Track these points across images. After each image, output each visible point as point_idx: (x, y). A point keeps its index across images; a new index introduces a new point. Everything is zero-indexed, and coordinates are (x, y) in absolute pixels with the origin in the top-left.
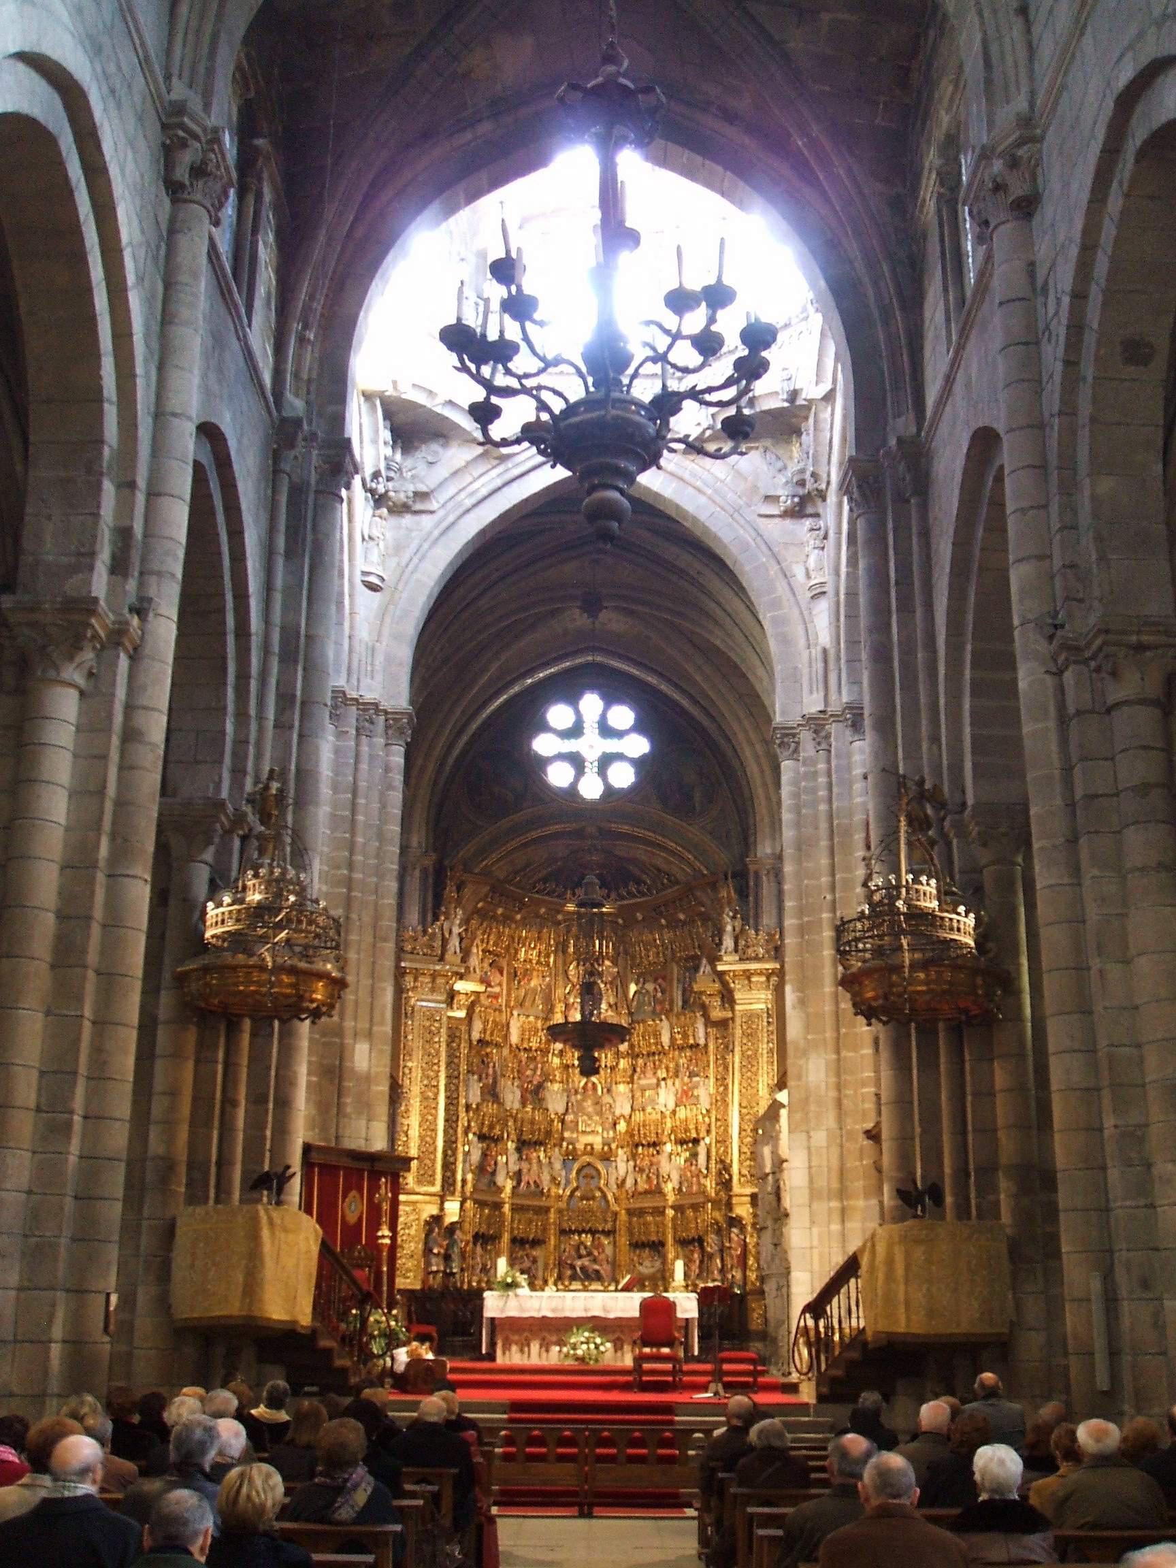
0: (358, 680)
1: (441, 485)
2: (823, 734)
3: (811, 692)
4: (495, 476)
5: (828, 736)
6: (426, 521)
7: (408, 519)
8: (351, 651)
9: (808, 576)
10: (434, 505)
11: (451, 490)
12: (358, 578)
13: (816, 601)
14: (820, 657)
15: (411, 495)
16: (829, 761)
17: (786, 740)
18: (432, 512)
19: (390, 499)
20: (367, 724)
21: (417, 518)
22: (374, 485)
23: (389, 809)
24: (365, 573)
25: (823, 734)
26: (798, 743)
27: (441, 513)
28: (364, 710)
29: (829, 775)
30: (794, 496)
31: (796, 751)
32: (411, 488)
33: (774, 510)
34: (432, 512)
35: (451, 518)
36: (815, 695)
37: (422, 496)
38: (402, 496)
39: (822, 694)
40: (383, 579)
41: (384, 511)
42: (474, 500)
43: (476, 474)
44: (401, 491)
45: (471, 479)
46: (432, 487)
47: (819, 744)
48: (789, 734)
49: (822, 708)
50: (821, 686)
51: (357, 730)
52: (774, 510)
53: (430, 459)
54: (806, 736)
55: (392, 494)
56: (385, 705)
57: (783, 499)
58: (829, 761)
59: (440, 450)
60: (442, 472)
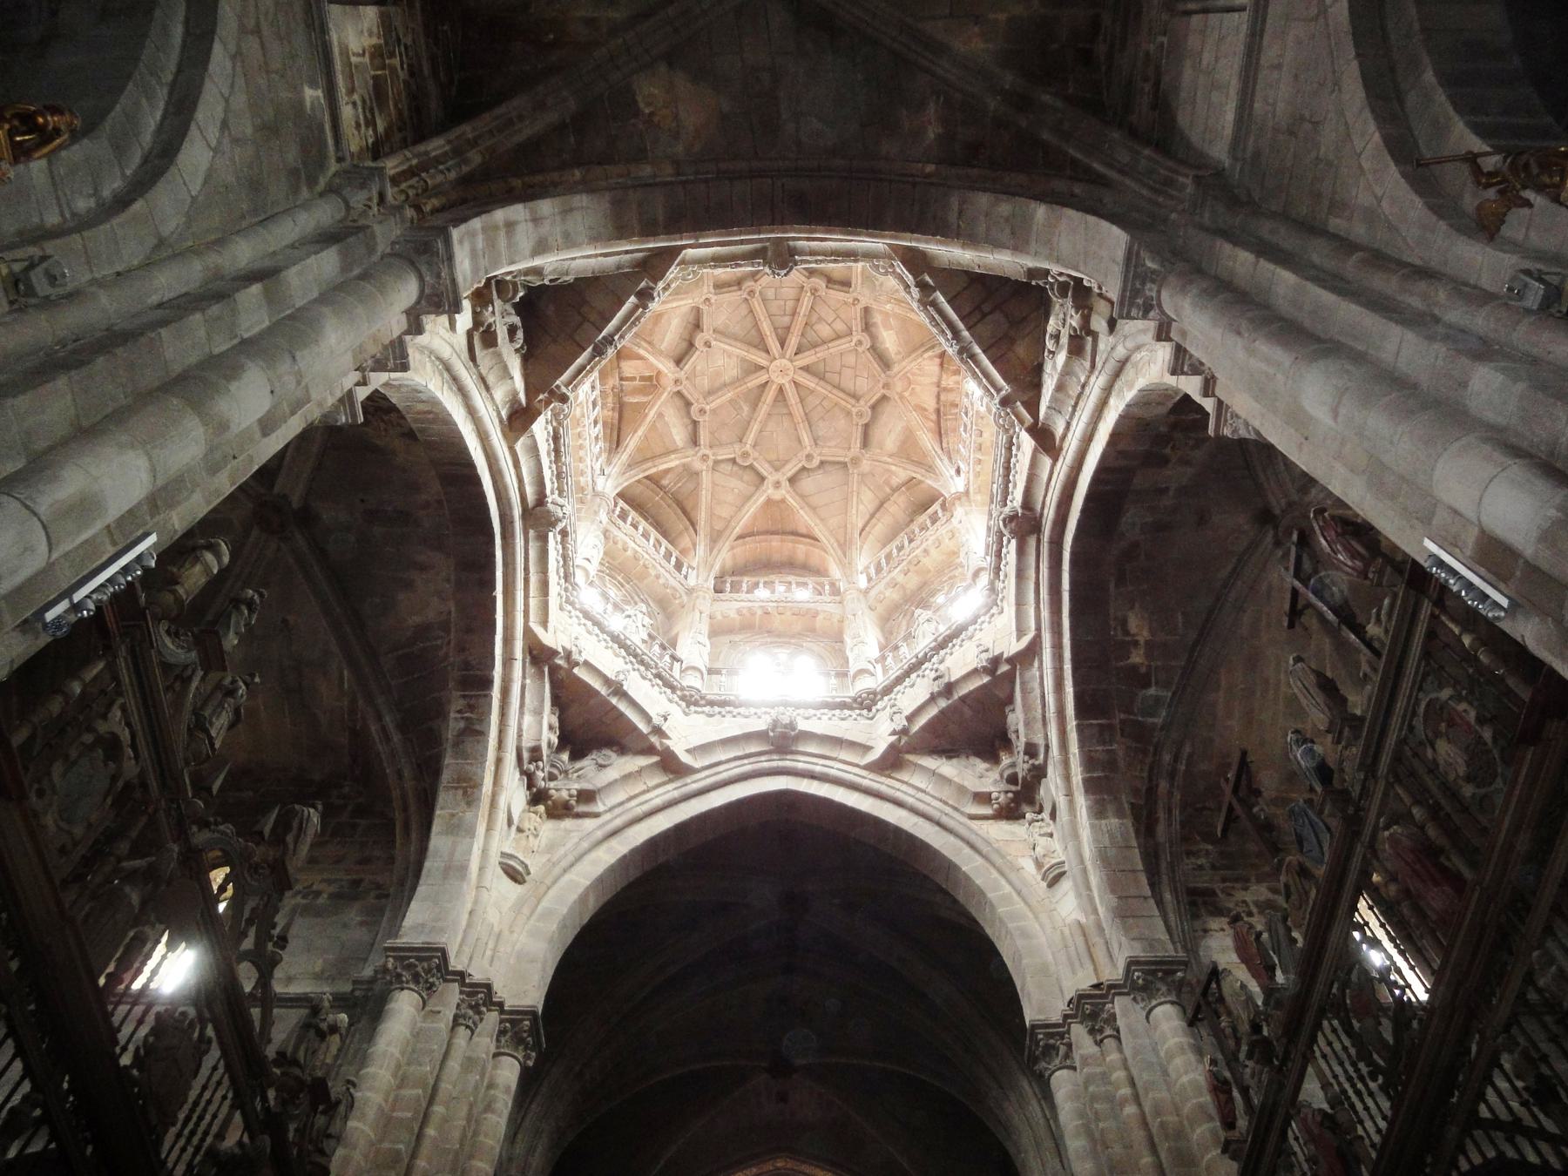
0: (471, 958)
1: (610, 785)
2: (1105, 1015)
3: (1074, 972)
4: (671, 791)
5: (1113, 1017)
6: (589, 824)
7: (568, 823)
8: (469, 925)
9: (1039, 865)
10: (599, 807)
11: (620, 796)
12: (494, 859)
13: (1056, 886)
14: (1078, 933)
15: (575, 793)
16: (1120, 1050)
17: (1052, 1041)
18: (597, 815)
19: (549, 797)
20: (470, 1012)
21: (580, 821)
22: (532, 767)
23: (481, 1138)
24: (503, 855)
25: (1105, 1015)
26: (1069, 1046)
27: (607, 817)
28: (469, 994)
29: (1126, 1068)
30: (1007, 792)
31: (1067, 1056)
32: (576, 786)
33: (988, 811)
34: (597, 815)
35: (618, 822)
36: (1080, 974)
37: (587, 796)
38: (565, 794)
39: (1091, 968)
40: (529, 873)
41: (541, 808)
42: (646, 808)
43: (651, 783)
44: (563, 790)
45: (645, 787)
46: (599, 785)
47: (1101, 1031)
48: (1058, 1032)
49: (1095, 982)
50: (1087, 961)
51: (456, 1017)
52: (988, 811)
53: (600, 761)
54: (1079, 1032)
55: (552, 792)
56: (502, 991)
57: (994, 795)
58: (1120, 1050)
59: (613, 755)
60: (612, 774)
